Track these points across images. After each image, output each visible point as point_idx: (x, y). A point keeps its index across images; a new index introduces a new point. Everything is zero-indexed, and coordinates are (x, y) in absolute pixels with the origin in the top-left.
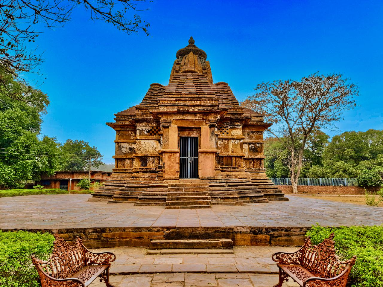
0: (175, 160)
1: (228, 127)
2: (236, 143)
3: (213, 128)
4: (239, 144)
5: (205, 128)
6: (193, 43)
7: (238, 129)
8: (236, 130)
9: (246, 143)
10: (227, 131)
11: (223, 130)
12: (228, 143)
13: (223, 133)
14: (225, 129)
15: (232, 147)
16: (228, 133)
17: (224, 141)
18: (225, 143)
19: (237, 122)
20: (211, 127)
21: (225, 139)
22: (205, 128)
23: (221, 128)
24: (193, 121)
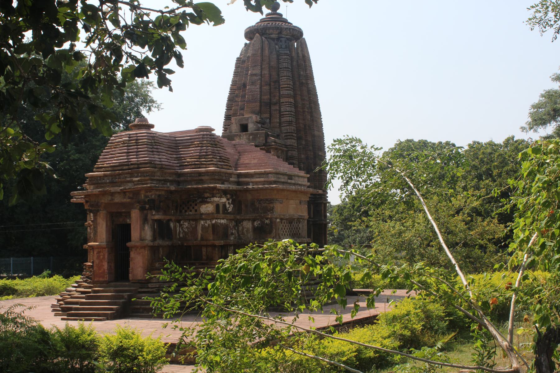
0: (104, 258)
1: (196, 200)
2: (207, 225)
3: (145, 212)
4: (211, 226)
5: (135, 214)
6: (278, 8)
7: (208, 202)
8: (207, 205)
9: (249, 220)
10: (196, 208)
11: (191, 205)
12: (196, 226)
13: (191, 211)
14: (193, 205)
15: (202, 230)
16: (196, 211)
17: (192, 222)
18: (193, 226)
19: (207, 193)
20: (142, 209)
21: (193, 220)
22: (135, 214)
23: (188, 202)
24: (122, 204)
